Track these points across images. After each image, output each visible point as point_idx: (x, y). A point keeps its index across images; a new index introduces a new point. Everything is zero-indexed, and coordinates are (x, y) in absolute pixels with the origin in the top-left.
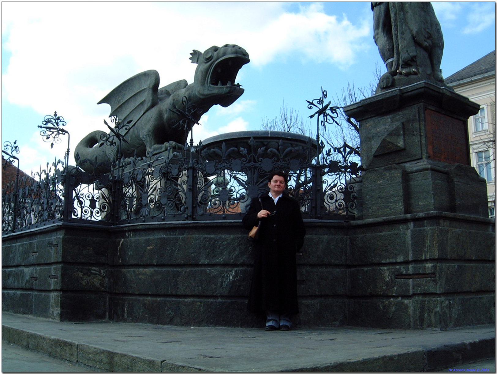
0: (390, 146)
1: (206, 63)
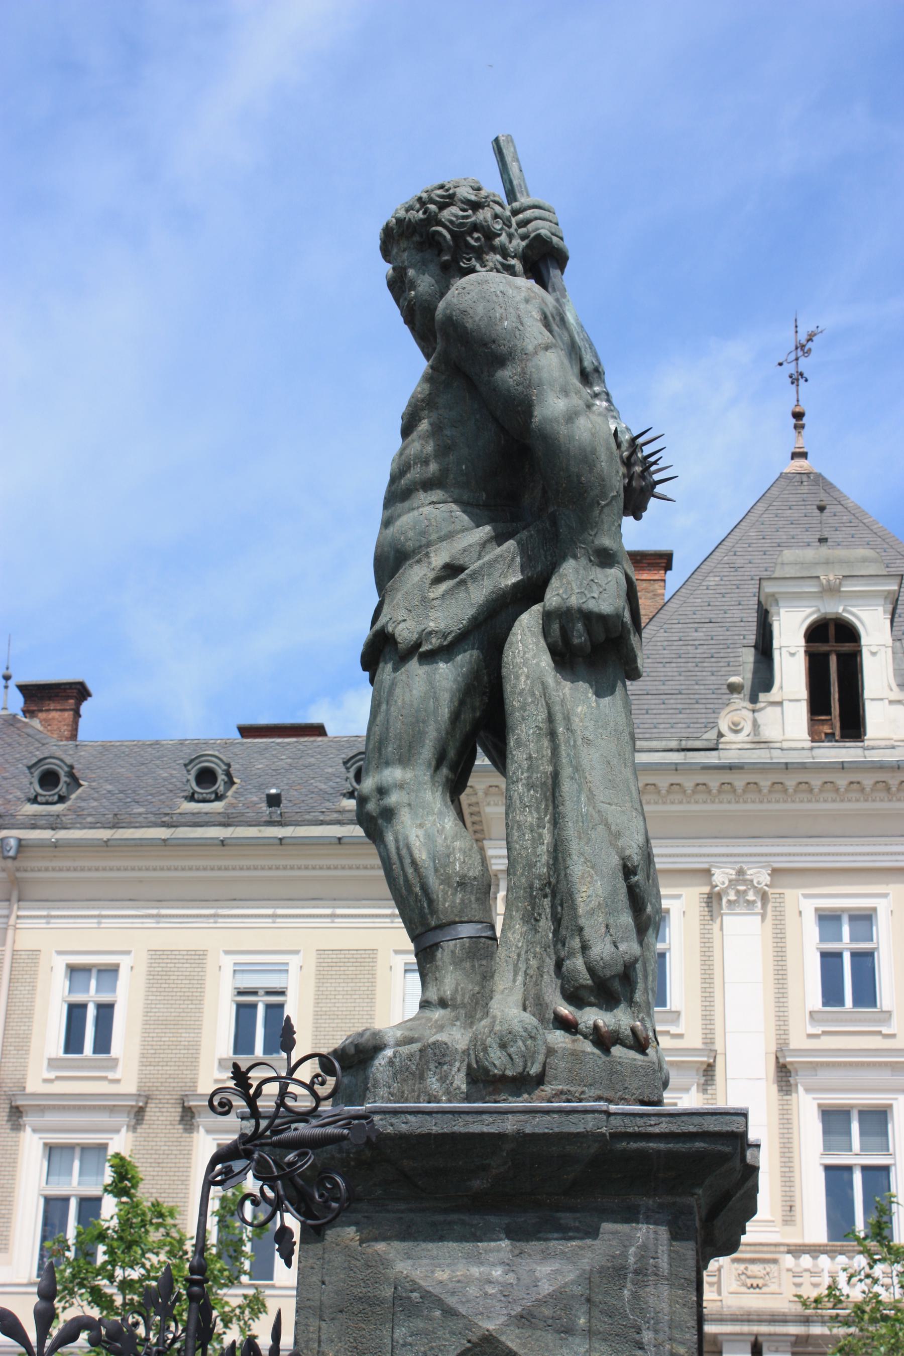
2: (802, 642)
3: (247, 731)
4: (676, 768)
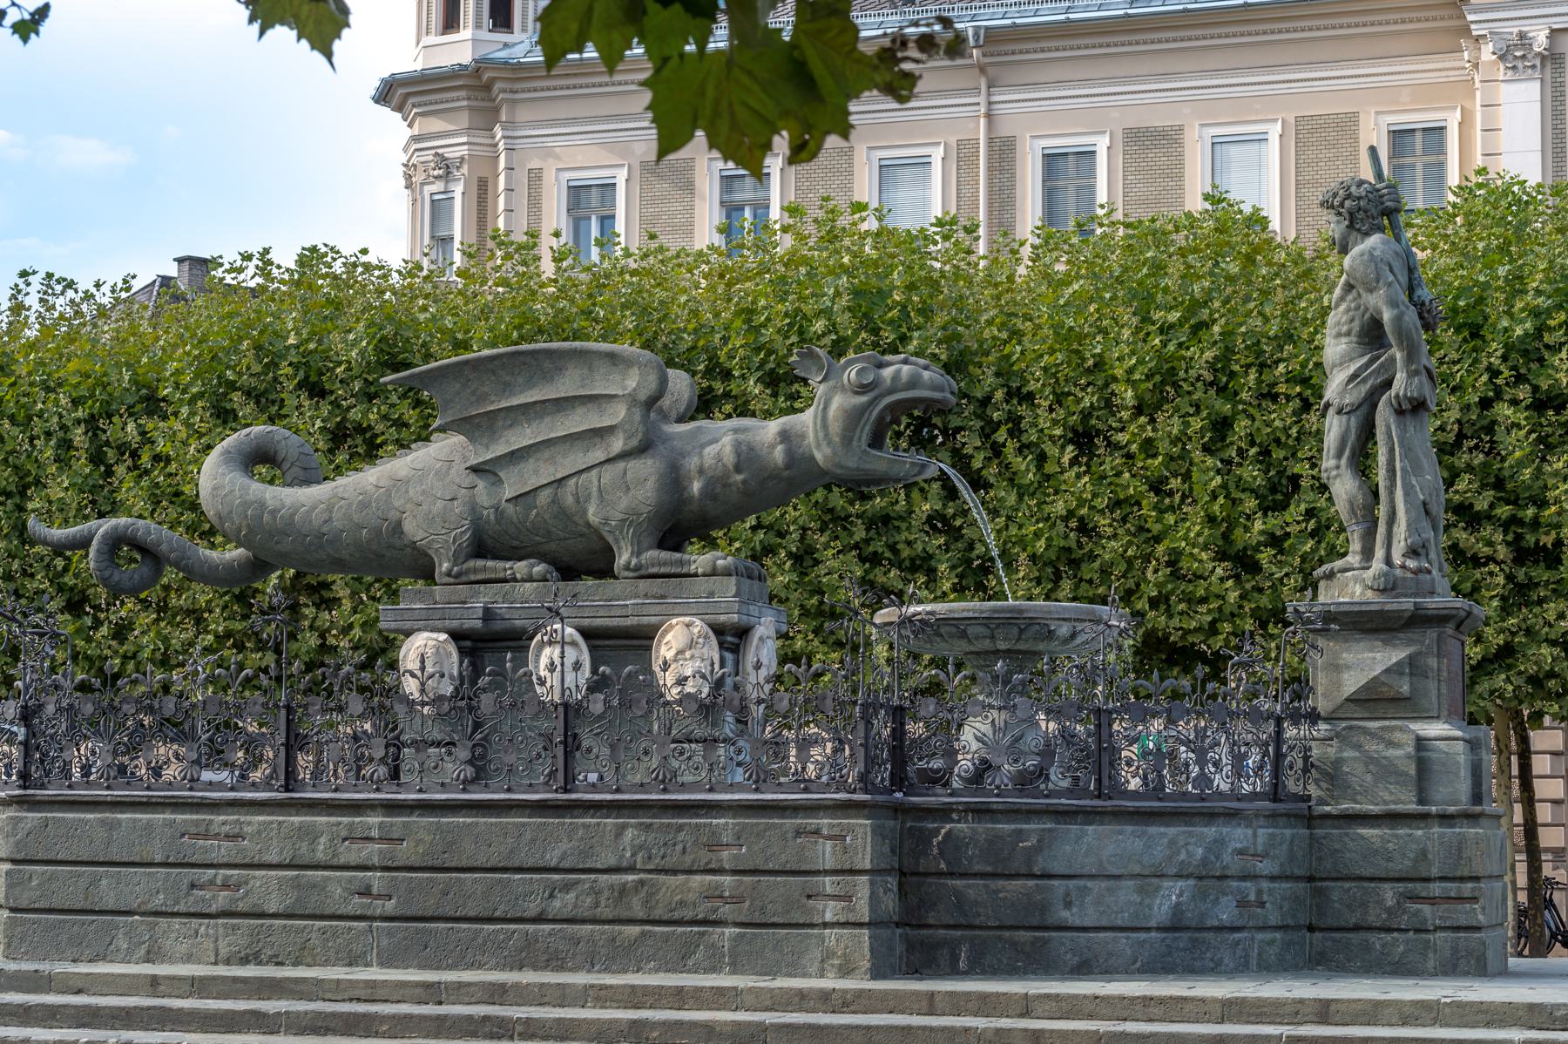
0: (1385, 689)
1: (857, 393)
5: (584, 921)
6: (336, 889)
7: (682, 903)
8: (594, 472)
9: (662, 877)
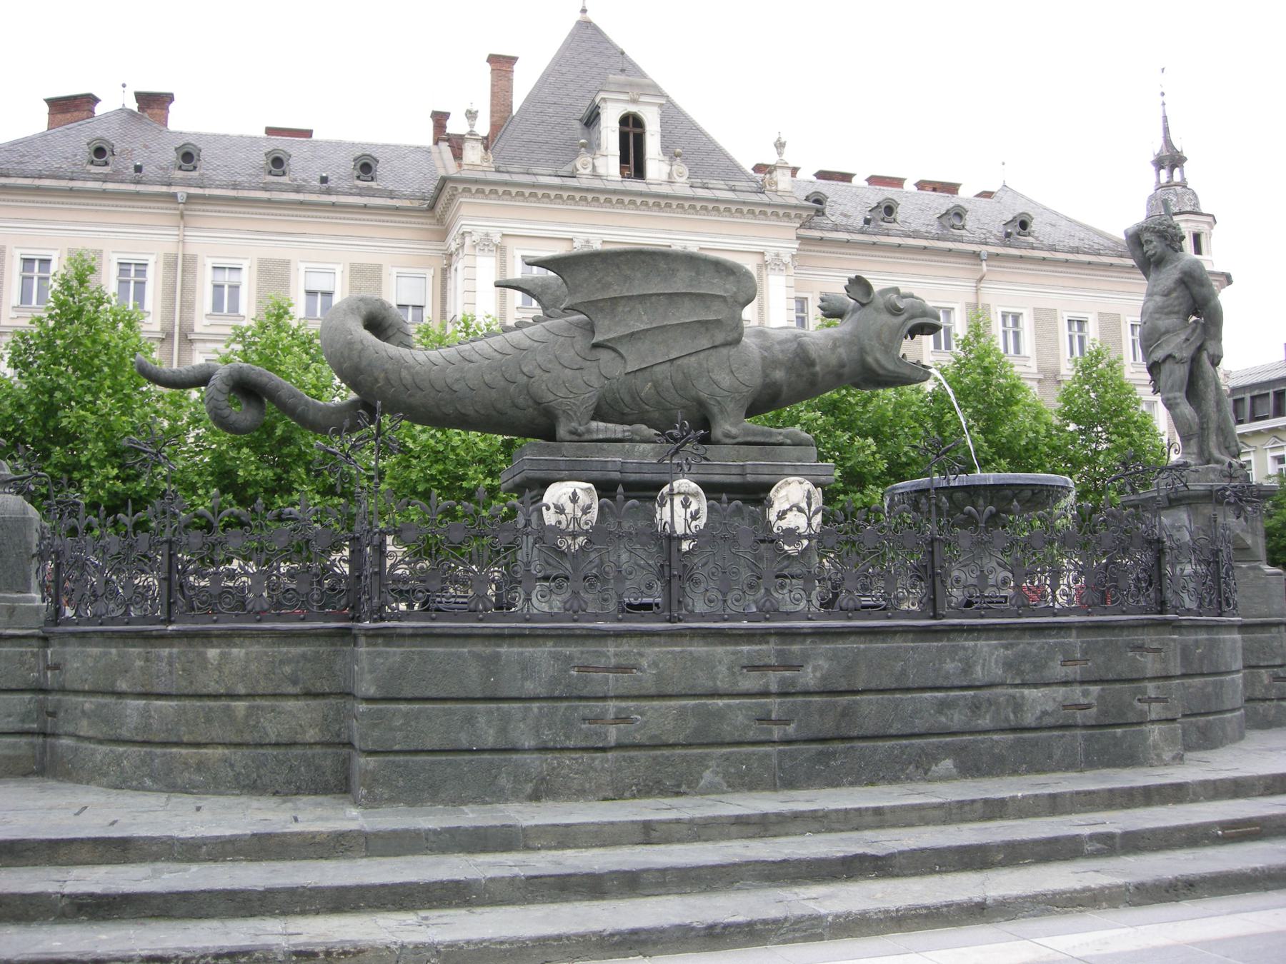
2: (618, 125)
3: (270, 131)
4: (561, 188)
5: (963, 733)
6: (737, 715)
7: (1045, 713)
8: (702, 355)
9: (1026, 691)
